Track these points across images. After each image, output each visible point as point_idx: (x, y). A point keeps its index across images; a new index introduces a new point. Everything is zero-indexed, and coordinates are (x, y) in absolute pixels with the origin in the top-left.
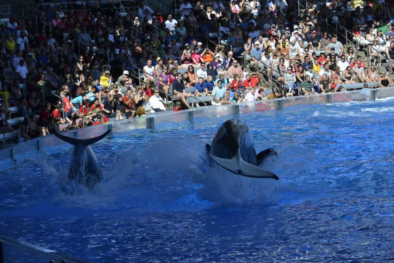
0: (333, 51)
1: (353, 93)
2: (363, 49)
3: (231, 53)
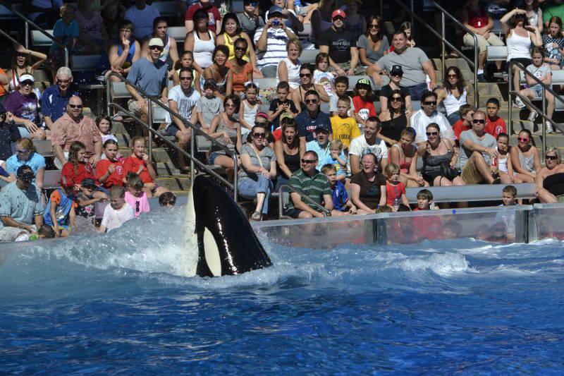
0: (396, 79)
2: (497, 75)
3: (64, 73)
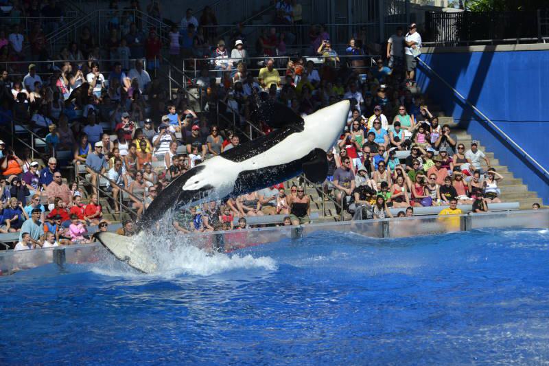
1: (262, 232)
3: (53, 160)
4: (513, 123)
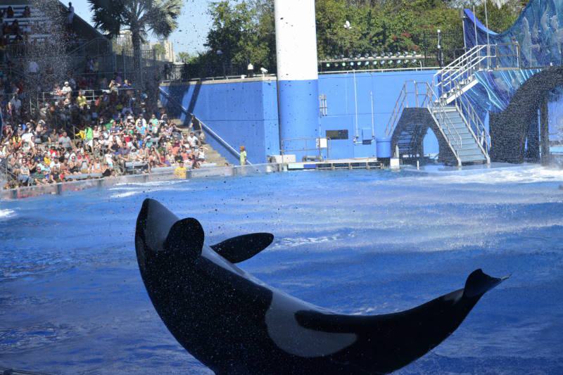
4: (211, 121)
